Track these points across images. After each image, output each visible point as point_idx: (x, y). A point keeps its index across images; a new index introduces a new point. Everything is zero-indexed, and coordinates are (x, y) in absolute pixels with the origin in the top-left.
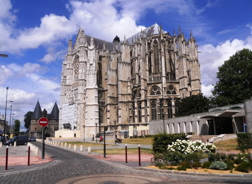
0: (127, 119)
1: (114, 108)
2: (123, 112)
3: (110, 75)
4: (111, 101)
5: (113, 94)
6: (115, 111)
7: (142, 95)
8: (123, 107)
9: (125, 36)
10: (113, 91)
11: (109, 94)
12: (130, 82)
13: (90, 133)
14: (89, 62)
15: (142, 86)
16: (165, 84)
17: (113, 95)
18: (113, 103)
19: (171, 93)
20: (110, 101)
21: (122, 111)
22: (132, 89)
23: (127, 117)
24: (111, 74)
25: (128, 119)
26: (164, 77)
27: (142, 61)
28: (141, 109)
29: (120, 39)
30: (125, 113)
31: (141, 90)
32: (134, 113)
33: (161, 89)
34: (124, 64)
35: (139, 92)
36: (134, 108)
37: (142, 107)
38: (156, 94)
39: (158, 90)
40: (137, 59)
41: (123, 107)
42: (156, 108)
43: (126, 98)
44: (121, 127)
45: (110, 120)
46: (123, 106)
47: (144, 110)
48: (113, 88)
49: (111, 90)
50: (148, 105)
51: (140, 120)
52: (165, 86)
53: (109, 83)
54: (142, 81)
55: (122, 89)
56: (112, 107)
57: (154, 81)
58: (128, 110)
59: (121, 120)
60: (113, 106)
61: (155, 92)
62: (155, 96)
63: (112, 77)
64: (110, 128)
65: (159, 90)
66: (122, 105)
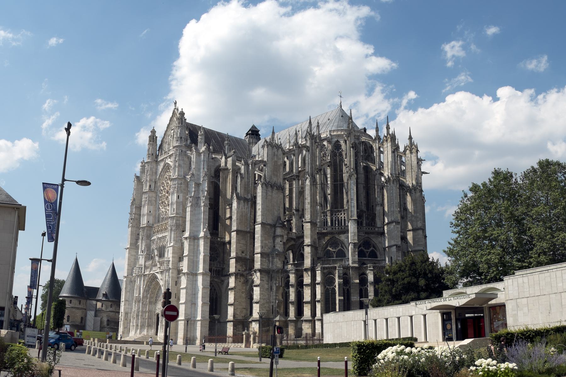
0: (271, 307)
2: (263, 292)
4: (239, 267)
5: (243, 252)
6: (246, 289)
7: (306, 257)
8: (263, 281)
10: (243, 245)
11: (234, 252)
12: (281, 228)
15: (307, 238)
16: (355, 235)
17: (244, 255)
19: (367, 254)
20: (236, 267)
21: (262, 290)
22: (284, 244)
23: (272, 304)
24: (241, 208)
25: (274, 309)
28: (303, 288)
29: (260, 133)
30: (267, 296)
31: (305, 245)
32: (286, 295)
34: (270, 189)
35: (300, 250)
36: (287, 285)
37: (304, 283)
38: (335, 256)
39: (340, 248)
40: (297, 179)
41: (263, 281)
43: (272, 263)
44: (258, 325)
45: (234, 310)
46: (263, 279)
47: (308, 289)
49: (239, 243)
50: (319, 279)
51: (300, 312)
52: (355, 239)
54: (307, 226)
55: (264, 242)
56: (240, 281)
57: (333, 229)
60: (242, 280)
62: (332, 260)
65: (342, 247)
66: (263, 277)
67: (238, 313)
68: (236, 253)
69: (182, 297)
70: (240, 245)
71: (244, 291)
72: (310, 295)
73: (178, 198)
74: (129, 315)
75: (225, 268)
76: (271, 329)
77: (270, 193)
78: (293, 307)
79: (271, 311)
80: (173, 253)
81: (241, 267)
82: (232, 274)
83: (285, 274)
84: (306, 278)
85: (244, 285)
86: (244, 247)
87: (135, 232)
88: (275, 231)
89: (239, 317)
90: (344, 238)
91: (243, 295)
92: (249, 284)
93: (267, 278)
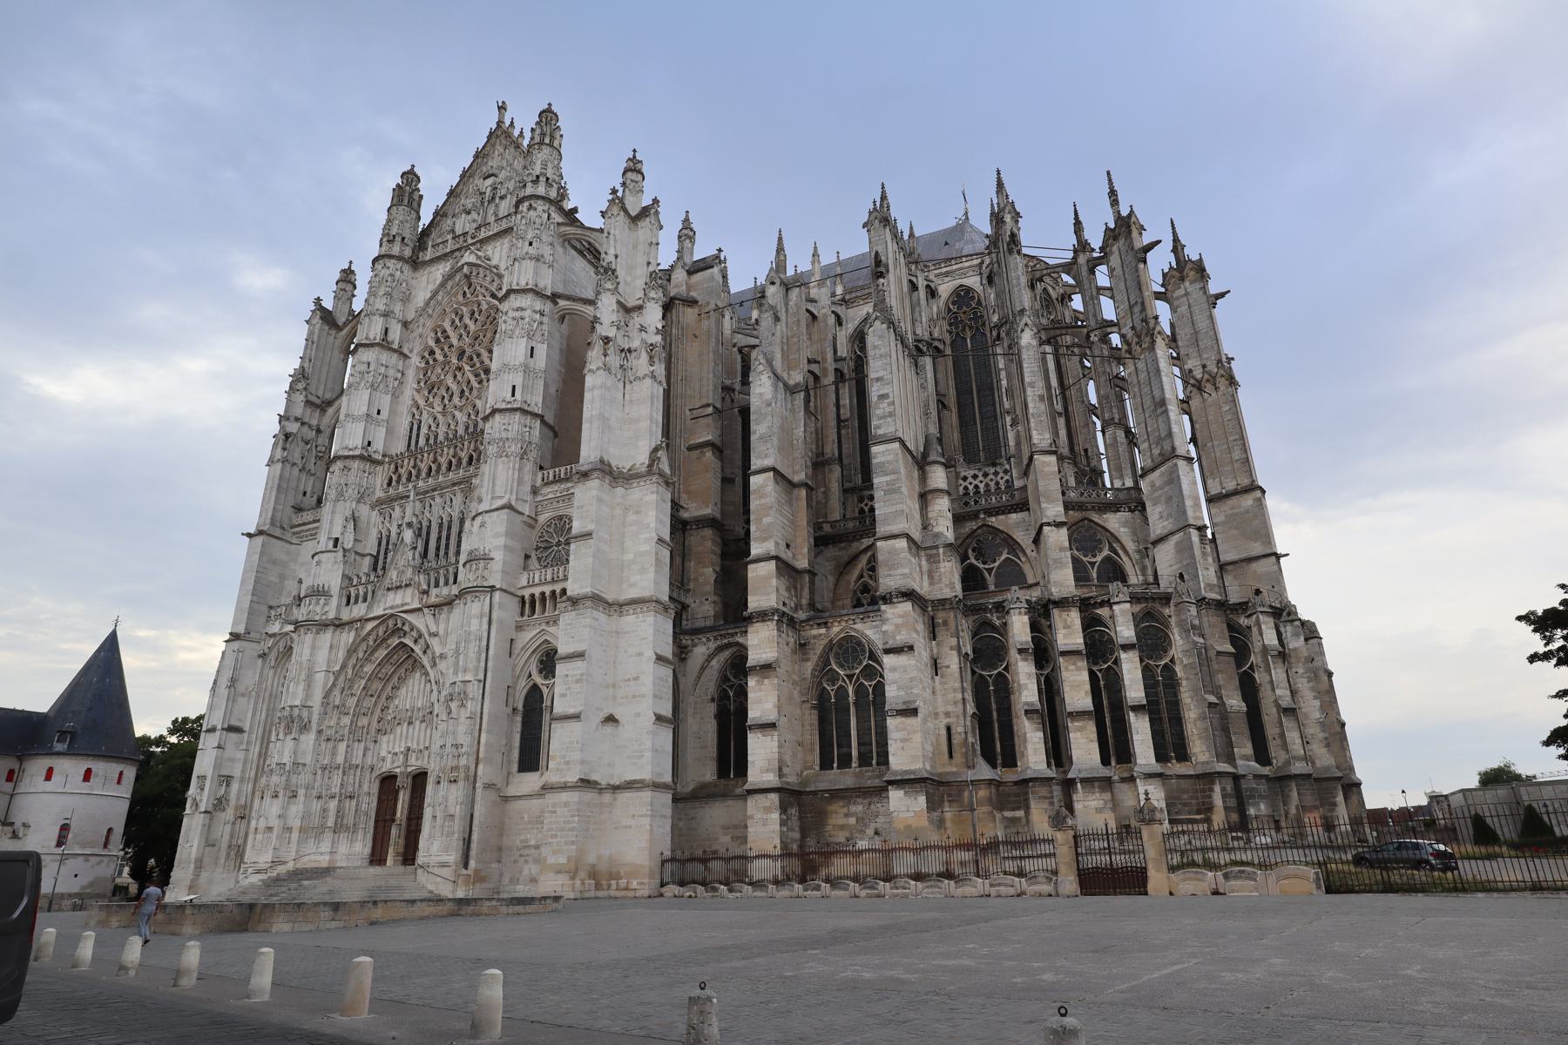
0: (944, 732)
1: (794, 652)
3: (773, 404)
5: (788, 546)
7: (1055, 561)
9: (883, 188)
11: (764, 539)
13: (591, 859)
14: (615, 291)
18: (790, 613)
23: (946, 721)
25: (956, 740)
26: (1185, 462)
27: (1034, 343)
33: (1126, 552)
38: (1095, 575)
39: (1106, 552)
41: (917, 632)
42: (1172, 660)
43: (931, 577)
44: (922, 799)
45: (780, 747)
47: (1078, 669)
48: (790, 502)
50: (1125, 631)
53: (768, 462)
54: (1048, 464)
58: (952, 662)
59: (917, 738)
61: (1093, 564)
63: (782, 427)
64: (783, 809)
65: (1112, 549)
67: (787, 758)
68: (777, 544)
69: (563, 695)
70: (781, 518)
71: (796, 678)
72: (1088, 687)
73: (532, 356)
74: (235, 786)
75: (688, 606)
76: (948, 815)
77: (901, 357)
78: (1038, 730)
79: (945, 748)
80: (508, 534)
81: (787, 595)
82: (763, 616)
83: (971, 619)
84: (1063, 631)
85: (796, 657)
86: (790, 530)
87: (293, 484)
88: (923, 478)
89: (792, 779)
90: (1117, 525)
91: (796, 692)
92: (814, 658)
93: (922, 626)
